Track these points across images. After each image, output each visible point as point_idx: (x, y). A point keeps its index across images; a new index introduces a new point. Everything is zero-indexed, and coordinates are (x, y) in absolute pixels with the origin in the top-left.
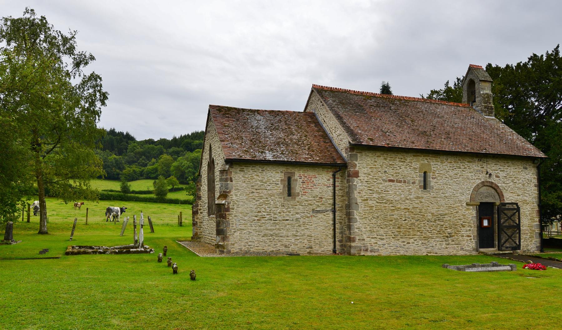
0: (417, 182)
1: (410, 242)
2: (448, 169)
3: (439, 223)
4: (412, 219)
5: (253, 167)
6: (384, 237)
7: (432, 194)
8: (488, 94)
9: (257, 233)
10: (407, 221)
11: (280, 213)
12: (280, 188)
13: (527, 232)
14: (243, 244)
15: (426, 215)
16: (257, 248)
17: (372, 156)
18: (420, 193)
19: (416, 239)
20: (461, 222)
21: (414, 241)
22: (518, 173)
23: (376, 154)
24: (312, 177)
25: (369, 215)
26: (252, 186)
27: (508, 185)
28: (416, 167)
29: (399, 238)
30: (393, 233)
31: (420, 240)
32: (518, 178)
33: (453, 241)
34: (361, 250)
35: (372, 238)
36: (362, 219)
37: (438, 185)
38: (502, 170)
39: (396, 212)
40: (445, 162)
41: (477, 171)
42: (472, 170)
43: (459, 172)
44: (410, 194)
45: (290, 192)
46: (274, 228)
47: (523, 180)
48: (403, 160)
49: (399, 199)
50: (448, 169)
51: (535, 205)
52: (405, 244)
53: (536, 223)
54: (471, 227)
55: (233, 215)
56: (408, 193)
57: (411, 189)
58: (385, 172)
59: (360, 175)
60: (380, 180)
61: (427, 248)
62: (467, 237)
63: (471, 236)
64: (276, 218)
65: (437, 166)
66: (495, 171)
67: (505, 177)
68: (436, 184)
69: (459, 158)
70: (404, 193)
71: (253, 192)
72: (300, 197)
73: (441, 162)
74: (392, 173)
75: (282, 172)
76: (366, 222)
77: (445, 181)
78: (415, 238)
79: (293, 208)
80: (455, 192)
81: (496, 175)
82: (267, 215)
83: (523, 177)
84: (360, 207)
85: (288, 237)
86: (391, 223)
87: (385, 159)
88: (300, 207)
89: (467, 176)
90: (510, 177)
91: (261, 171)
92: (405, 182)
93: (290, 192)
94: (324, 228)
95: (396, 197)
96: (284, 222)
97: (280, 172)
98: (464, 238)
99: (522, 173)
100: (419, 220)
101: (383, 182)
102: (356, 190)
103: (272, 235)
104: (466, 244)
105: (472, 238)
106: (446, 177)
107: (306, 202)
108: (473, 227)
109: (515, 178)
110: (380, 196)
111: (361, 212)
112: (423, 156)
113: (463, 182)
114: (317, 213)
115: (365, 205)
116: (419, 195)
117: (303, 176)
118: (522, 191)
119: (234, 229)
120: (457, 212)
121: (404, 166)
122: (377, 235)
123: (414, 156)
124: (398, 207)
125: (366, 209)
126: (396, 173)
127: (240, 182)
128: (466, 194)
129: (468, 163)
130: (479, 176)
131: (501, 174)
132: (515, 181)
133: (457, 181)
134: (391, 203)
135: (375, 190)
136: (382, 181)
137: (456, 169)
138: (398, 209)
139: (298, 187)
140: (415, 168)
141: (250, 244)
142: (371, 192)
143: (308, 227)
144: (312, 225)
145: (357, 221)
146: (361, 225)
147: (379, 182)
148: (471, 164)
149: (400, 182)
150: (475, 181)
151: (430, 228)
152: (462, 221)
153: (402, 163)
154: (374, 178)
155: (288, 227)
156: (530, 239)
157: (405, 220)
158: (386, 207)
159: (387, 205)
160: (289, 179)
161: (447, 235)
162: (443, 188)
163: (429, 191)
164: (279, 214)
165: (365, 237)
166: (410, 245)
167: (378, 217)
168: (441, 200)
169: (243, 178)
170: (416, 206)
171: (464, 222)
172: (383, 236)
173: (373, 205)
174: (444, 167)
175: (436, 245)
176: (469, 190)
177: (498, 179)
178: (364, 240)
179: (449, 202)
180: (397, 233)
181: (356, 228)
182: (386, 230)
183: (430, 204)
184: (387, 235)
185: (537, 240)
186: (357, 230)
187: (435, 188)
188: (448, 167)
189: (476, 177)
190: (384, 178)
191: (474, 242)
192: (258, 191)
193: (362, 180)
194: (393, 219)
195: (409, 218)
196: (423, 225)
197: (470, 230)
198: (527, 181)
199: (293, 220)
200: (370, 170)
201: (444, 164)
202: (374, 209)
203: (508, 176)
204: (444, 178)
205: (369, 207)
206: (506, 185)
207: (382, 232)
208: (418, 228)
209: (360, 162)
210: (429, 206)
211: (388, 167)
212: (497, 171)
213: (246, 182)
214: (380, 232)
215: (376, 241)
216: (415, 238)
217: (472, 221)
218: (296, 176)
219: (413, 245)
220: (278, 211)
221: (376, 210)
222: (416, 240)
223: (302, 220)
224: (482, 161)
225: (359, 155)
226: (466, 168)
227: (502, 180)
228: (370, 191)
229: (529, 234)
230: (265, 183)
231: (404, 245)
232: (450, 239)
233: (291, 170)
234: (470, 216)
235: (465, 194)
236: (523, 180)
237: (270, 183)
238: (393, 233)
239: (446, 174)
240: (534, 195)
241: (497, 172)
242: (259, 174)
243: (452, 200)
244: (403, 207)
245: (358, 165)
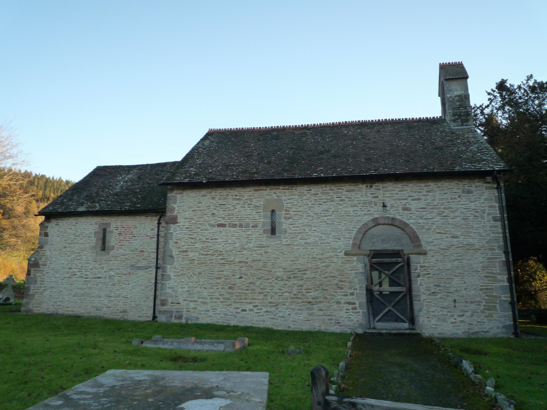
0: (260, 225)
1: (247, 309)
2: (312, 204)
3: (295, 282)
4: (252, 276)
5: (67, 220)
6: (208, 301)
7: (284, 240)
8: (460, 96)
9: (69, 292)
10: (243, 279)
11: (91, 269)
12: (93, 241)
13: (478, 299)
14: (51, 303)
15: (273, 270)
16: (66, 309)
17: (196, 195)
18: (265, 240)
19: (256, 304)
20: (335, 282)
21: (252, 308)
22: (452, 201)
23: (200, 193)
24: (131, 228)
25: (189, 271)
26: (65, 241)
27: (431, 220)
28: (258, 204)
29: (230, 303)
30: (221, 295)
31: (263, 306)
32: (452, 208)
33: (321, 310)
34: (172, 317)
35: (190, 301)
36: (179, 276)
37: (294, 227)
38: (416, 197)
39: (227, 267)
40: (305, 195)
41: (365, 203)
42: (355, 202)
43: (331, 207)
44: (249, 241)
45: (104, 246)
46: (85, 286)
47: (463, 210)
48: (238, 197)
49: (231, 249)
50: (312, 204)
51: (497, 251)
52: (239, 311)
53: (501, 284)
54: (354, 289)
55: (44, 272)
56: (246, 240)
57: (251, 235)
58: (213, 214)
59: (179, 220)
60: (206, 226)
61: (273, 319)
62: (347, 305)
63: (354, 304)
64: (87, 275)
65: (292, 201)
66: (401, 201)
68: (291, 226)
69: (330, 187)
70: (239, 240)
71: (65, 247)
72: (115, 251)
73: (299, 195)
74: (223, 216)
75: (96, 224)
76: (183, 280)
77: (307, 221)
78: (255, 303)
79: (106, 263)
80: (323, 236)
81: (402, 208)
82: (79, 271)
83: (463, 206)
84: (176, 260)
85: (100, 297)
86: (219, 281)
87: (213, 198)
88: (116, 262)
89: (345, 211)
90: (432, 208)
91: (74, 224)
92: (241, 226)
93: (104, 246)
94: (144, 288)
95: (228, 247)
96: (96, 280)
97: (94, 223)
98: (342, 305)
99: (459, 199)
100: (262, 277)
101: (209, 228)
102: (172, 239)
103: (82, 295)
104: (345, 315)
105: (357, 306)
106: (309, 216)
107: (122, 257)
108: (358, 290)
109: (444, 208)
110: (204, 246)
111: (177, 266)
112: (270, 190)
113: (338, 221)
114: (137, 269)
115: (184, 258)
116: (263, 243)
117: (120, 227)
118: (463, 230)
119: (45, 287)
120: (327, 266)
121: (240, 206)
122: (198, 298)
123: (254, 190)
124: (230, 259)
125: (185, 262)
126: (229, 215)
127: (54, 237)
128: (345, 238)
129: (347, 193)
130: (369, 211)
131: (414, 205)
132: (445, 214)
133: (328, 219)
134: (220, 255)
135: (198, 238)
136: (208, 226)
137: (328, 203)
138: (230, 263)
139: (112, 240)
140: (256, 207)
141: (59, 303)
142: (193, 241)
143: (124, 286)
144: (129, 284)
145: (170, 279)
146: (176, 284)
147: (204, 227)
148: (353, 193)
149: (235, 226)
150: (360, 217)
151: (280, 289)
152: (337, 279)
153: (237, 202)
154: (198, 222)
155: (100, 285)
156: (488, 312)
157: (241, 278)
158: (212, 260)
159: (214, 258)
160: (105, 230)
161: (310, 300)
162: (302, 231)
163: (280, 237)
164: (91, 271)
165: (181, 300)
166: (246, 313)
167: (200, 273)
168: (299, 249)
169: (58, 233)
170: (259, 257)
171: (340, 281)
172: (206, 299)
173: (195, 258)
174: (305, 202)
175: (289, 314)
176: (350, 233)
177: (409, 212)
178: (179, 303)
179: (313, 251)
180: (227, 296)
181: (169, 288)
182: (211, 290)
183: (281, 254)
184: (212, 298)
185: (506, 314)
186: (170, 291)
187: (289, 231)
188: (311, 201)
190: (212, 222)
191: (361, 314)
192: (71, 245)
193: (181, 227)
194: (222, 276)
195: (246, 275)
196: (268, 285)
197: (352, 294)
198: (473, 213)
199: (105, 278)
200: (193, 213)
201: (304, 198)
202: (196, 262)
203: (429, 207)
204: (304, 217)
205: (190, 260)
206: (425, 221)
207: (205, 294)
208: (261, 289)
209: (180, 205)
210: (278, 258)
211: (218, 208)
212: (406, 201)
213: (60, 237)
214: (202, 294)
215: (195, 306)
216: (255, 303)
217: (356, 280)
218: (112, 227)
219: (252, 313)
220: (90, 267)
221: (198, 263)
222: (257, 306)
223: (116, 278)
224: (374, 187)
225: (178, 196)
226: (344, 200)
227: (418, 213)
228: (191, 240)
229: (484, 303)
230: (78, 236)
231: (236, 312)
232: (315, 306)
233: (107, 220)
234: (353, 272)
235: (342, 239)
236: (463, 210)
237: (83, 237)
238: (221, 295)
239: (309, 212)
240: (492, 235)
241: (404, 202)
242: (73, 227)
243: (319, 248)
244: (237, 260)
245: (177, 209)
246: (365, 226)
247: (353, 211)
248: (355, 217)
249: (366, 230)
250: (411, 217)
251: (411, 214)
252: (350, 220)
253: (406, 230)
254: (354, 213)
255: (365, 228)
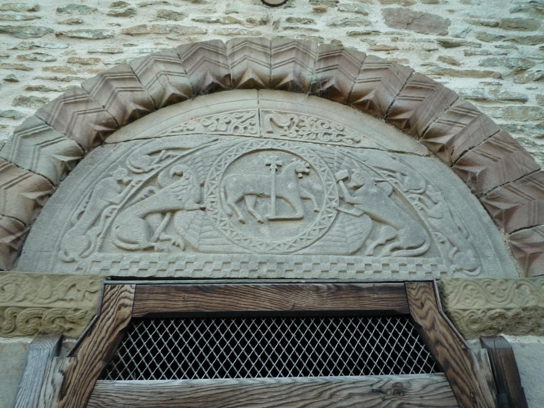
67: (519, 26)
150: (100, 46)
177: (433, 37)
189: (127, 23)
227: (488, 46)
246: (115, 85)
247: (59, 10)
248: (60, 44)
249: (113, 112)
250: (454, 64)
251: (447, 45)
252: (15, 55)
253: (433, 125)
254: (64, 17)
255: (114, 96)
